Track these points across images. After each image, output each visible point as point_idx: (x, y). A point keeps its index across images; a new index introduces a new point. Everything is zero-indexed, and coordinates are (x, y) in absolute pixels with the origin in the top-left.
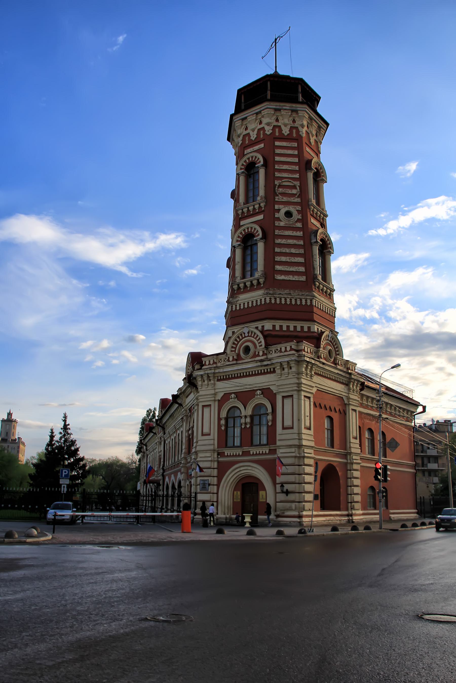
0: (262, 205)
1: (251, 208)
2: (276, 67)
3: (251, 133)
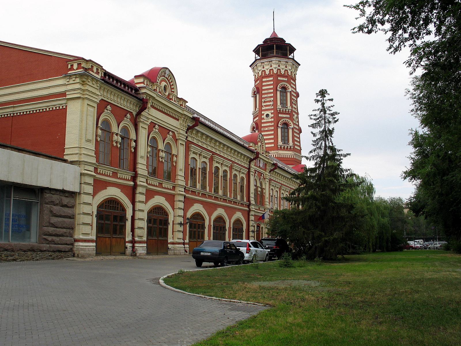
0: (290, 111)
1: (284, 110)
2: (274, 29)
3: (281, 70)
